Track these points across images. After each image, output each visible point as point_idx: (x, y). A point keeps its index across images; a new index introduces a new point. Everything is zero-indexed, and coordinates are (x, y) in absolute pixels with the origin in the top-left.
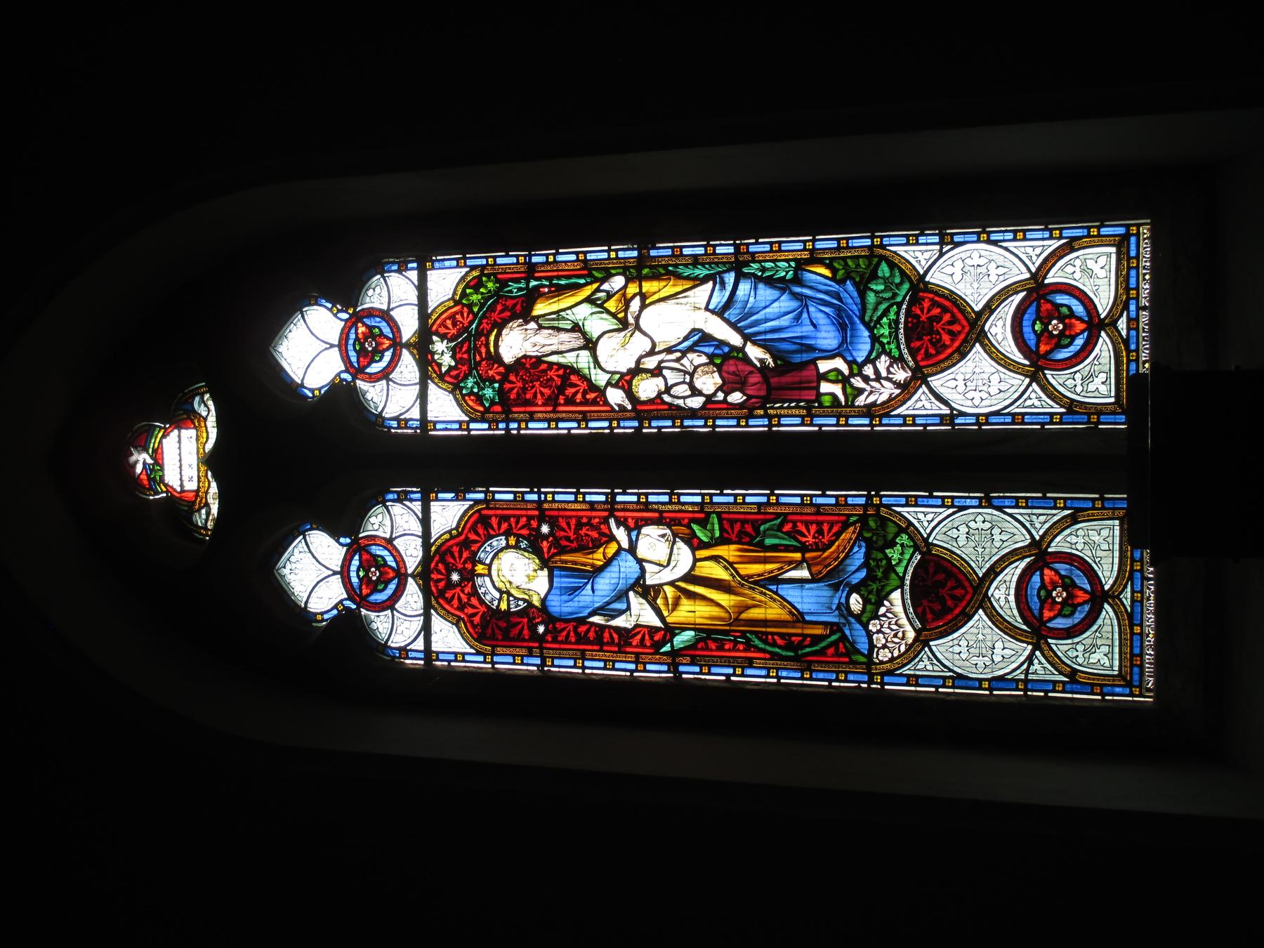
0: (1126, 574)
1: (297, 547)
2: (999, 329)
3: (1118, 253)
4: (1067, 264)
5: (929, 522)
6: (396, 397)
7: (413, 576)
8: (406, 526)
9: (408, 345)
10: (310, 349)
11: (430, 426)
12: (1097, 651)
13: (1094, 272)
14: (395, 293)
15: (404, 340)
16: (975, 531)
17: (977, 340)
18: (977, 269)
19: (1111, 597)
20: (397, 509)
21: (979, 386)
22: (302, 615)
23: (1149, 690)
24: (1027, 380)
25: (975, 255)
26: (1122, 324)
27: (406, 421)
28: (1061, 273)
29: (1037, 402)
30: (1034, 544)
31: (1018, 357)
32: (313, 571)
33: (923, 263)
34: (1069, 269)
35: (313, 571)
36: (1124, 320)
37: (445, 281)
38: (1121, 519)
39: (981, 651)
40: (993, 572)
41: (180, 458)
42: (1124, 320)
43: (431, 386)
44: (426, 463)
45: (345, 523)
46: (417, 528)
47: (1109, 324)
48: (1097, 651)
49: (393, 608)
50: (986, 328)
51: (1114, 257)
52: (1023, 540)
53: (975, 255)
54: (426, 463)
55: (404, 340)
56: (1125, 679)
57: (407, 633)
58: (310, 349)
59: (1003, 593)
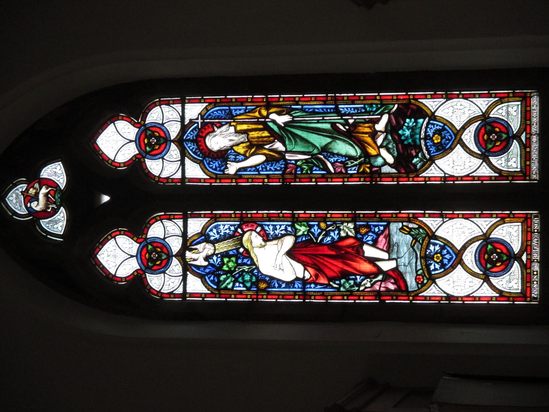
0: (526, 247)
1: (111, 244)
2: (468, 137)
3: (521, 104)
4: (499, 109)
5: (437, 225)
6: (165, 167)
7: (176, 256)
8: (173, 232)
9: (173, 141)
10: (117, 142)
11: (186, 180)
12: (511, 281)
13: (510, 113)
14: (166, 116)
15: (172, 139)
16: (458, 230)
17: (458, 143)
18: (458, 110)
19: (518, 257)
20: (167, 223)
21: (458, 164)
22: (111, 278)
23: (534, 298)
24: (481, 161)
25: (459, 104)
26: (523, 137)
27: (173, 179)
28: (496, 113)
29: (485, 171)
30: (484, 235)
31: (476, 150)
32: (118, 256)
33: (434, 107)
34: (500, 111)
35: (118, 256)
36: (524, 134)
37: (194, 110)
38: (522, 223)
39: (460, 284)
40: (464, 248)
41: (41, 198)
42: (524, 134)
43: (187, 161)
44: (181, 199)
45: (137, 231)
46: (179, 232)
47: (517, 137)
48: (511, 281)
49: (164, 272)
50: (462, 137)
51: (520, 106)
52: (478, 233)
53: (459, 104)
54: (181, 199)
55: (172, 139)
56: (524, 294)
57: (172, 285)
58: (117, 142)
59: (469, 257)
